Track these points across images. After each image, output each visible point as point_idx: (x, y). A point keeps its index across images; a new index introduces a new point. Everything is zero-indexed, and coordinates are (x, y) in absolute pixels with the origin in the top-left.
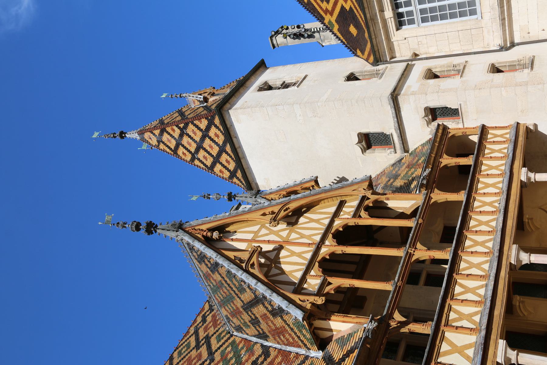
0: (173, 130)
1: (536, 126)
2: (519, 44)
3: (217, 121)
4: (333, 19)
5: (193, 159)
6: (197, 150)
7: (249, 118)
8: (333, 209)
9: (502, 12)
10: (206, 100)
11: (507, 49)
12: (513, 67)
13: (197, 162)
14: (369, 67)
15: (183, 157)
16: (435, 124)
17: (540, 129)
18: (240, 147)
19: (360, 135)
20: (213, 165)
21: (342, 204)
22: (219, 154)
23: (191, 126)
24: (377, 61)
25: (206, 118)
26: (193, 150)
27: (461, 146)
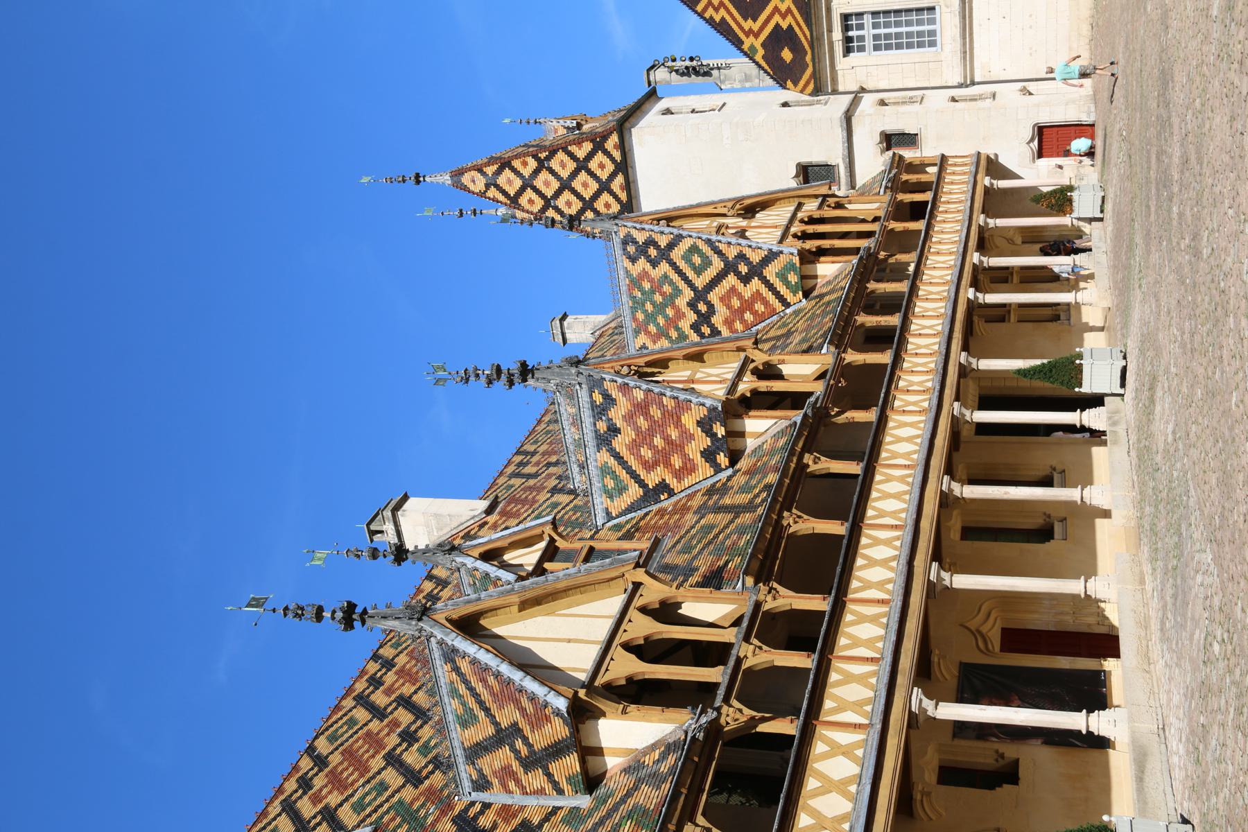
0: (525, 164)
1: (996, 156)
2: (979, 83)
4: (758, 43)
6: (558, 194)
8: (792, 208)
9: (964, 44)
10: (579, 126)
11: (967, 86)
12: (973, 99)
14: (806, 98)
15: (527, 207)
16: (890, 153)
17: (1001, 160)
18: (635, 181)
19: (798, 165)
21: (800, 206)
22: (596, 196)
23: (561, 155)
24: (817, 91)
25: (592, 141)
26: (549, 193)
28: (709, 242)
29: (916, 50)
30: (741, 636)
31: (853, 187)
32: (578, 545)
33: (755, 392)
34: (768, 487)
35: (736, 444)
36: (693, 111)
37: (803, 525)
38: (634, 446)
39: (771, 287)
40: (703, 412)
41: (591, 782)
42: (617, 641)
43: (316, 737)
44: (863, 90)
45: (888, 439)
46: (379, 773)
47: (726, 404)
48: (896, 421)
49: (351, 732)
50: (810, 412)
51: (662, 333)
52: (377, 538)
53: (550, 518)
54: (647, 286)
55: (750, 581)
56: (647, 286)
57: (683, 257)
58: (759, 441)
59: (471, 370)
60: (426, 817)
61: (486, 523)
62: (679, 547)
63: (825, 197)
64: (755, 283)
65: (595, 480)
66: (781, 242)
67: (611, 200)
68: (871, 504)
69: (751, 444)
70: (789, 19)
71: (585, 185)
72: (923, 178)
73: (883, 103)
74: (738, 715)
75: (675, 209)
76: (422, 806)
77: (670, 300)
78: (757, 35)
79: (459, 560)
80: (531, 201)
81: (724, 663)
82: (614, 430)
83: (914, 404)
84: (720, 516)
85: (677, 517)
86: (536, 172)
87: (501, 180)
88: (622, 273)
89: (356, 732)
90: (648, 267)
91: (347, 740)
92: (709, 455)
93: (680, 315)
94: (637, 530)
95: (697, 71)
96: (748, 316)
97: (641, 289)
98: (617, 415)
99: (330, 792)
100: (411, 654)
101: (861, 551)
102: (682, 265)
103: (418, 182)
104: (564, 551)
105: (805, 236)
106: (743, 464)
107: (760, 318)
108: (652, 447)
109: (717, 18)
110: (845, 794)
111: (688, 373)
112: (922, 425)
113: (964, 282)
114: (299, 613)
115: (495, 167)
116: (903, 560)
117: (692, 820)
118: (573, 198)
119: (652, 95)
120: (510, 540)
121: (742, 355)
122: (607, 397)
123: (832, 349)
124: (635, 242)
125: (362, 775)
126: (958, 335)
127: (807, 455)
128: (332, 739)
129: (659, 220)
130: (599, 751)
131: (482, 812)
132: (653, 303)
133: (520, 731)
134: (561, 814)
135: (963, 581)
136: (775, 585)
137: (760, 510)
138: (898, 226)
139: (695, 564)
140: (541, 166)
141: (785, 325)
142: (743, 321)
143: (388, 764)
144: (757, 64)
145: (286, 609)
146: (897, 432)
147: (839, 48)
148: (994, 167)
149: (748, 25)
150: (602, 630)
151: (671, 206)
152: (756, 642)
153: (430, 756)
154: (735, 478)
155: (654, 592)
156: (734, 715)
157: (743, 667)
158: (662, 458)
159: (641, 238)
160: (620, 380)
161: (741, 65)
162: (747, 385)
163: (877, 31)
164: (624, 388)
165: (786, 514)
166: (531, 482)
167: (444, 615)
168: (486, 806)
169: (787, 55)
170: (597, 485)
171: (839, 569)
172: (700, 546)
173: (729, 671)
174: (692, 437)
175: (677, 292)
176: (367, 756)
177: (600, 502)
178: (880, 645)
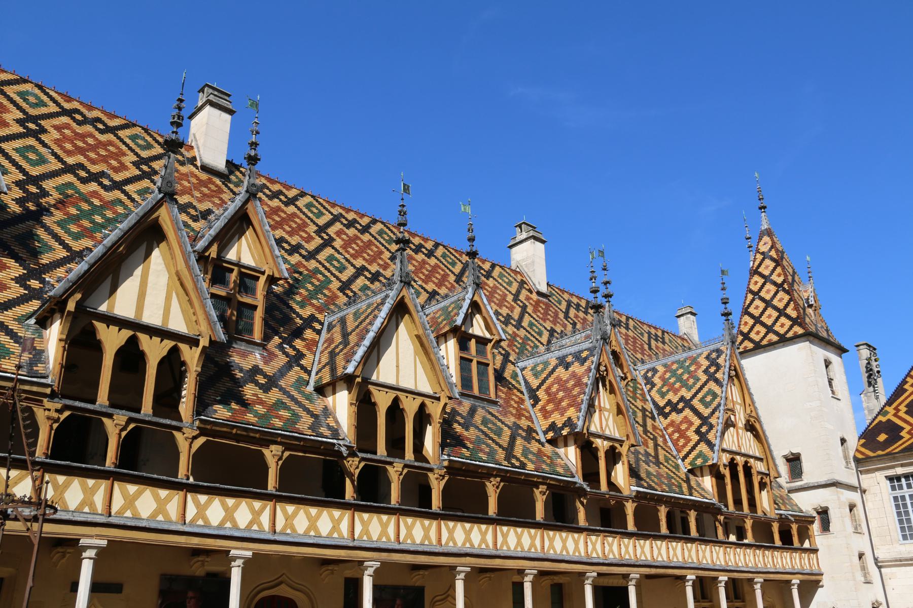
0: (779, 275)
1: (822, 586)
3: (798, 330)
4: (890, 416)
5: (751, 292)
6: (762, 299)
7: (802, 357)
8: (758, 455)
10: (810, 306)
12: (863, 568)
13: (750, 297)
14: (851, 454)
15: (753, 281)
16: (815, 514)
18: (775, 349)
20: (752, 316)
21: (761, 460)
22: (763, 325)
23: (787, 298)
24: (857, 461)
25: (798, 317)
26: (762, 294)
27: (804, 534)
28: (719, 405)
29: (898, 526)
30: (408, 463)
31: (789, 492)
32: (490, 356)
33: (597, 449)
34: (523, 466)
35: (561, 443)
36: (830, 381)
37: (492, 490)
38: (559, 380)
39: (693, 448)
40: (575, 420)
41: (321, 390)
42: (399, 393)
43: (382, 223)
44: (864, 492)
45: (564, 534)
46: (352, 265)
47: (580, 434)
48: (579, 538)
49: (384, 242)
50: (577, 485)
51: (665, 381)
52: (518, 229)
53: (504, 337)
54: (692, 368)
55: (446, 464)
56: (692, 368)
57: (710, 389)
58: (563, 456)
59: (595, 275)
60: (317, 299)
61: (530, 291)
62: (489, 417)
63: (768, 475)
64: (696, 438)
65: (541, 358)
66: (724, 450)
67: (762, 334)
68: (512, 529)
69: (561, 451)
70: (908, 436)
71: (770, 316)
72: (796, 539)
73: (852, 507)
74: (354, 467)
75: (745, 380)
76: (325, 295)
77: (684, 384)
78: (895, 415)
79: (470, 290)
80: (756, 283)
81: (388, 456)
82: (567, 366)
83: (594, 549)
84: (507, 439)
85: (514, 412)
86: (775, 283)
87: (768, 262)
88: (699, 351)
89: (383, 245)
90: (704, 368)
91: (378, 241)
92: (553, 427)
93: (676, 391)
94: (510, 389)
95: (871, 376)
96: (676, 435)
97: (691, 365)
98: (576, 368)
99: (343, 240)
100: (437, 266)
101: (476, 526)
102: (705, 389)
103: (760, 208)
104: (485, 349)
105: (732, 465)
106: (548, 448)
107: (675, 443)
108: (558, 390)
109: (906, 387)
110: (308, 529)
111: (608, 406)
112: (577, 554)
113: (700, 572)
114: (402, 213)
115: (775, 256)
116: (469, 551)
117: (286, 449)
118: (760, 310)
119: (841, 350)
120: (487, 317)
121: (625, 438)
122: (585, 359)
123: (634, 494)
124: (718, 357)
125: (352, 256)
126: (653, 571)
127: (545, 487)
128: (381, 233)
129: (735, 370)
130: (334, 393)
131: (314, 330)
132: (682, 374)
133: (345, 347)
134: (305, 376)
135: (460, 586)
136: (446, 478)
137: (506, 463)
138: (749, 524)
139: (472, 429)
140: (779, 286)
141: (667, 460)
142: (673, 432)
143: (358, 269)
144: (876, 417)
145: (403, 206)
146: (570, 539)
147: (891, 472)
148: (810, 586)
149: (903, 408)
150: (407, 383)
151: (748, 376)
152: (405, 471)
153: (359, 293)
154: (537, 444)
155: (435, 410)
156: (354, 465)
157: (388, 467)
158: (552, 398)
159: (721, 361)
160: (593, 367)
161: (876, 406)
162: (602, 445)
163: (907, 498)
164: (589, 370)
165: (498, 479)
166: (561, 315)
167: (405, 294)
168: (319, 332)
169: (882, 437)
170: (538, 360)
171: (459, 514)
172: (485, 429)
173: (383, 459)
174: (562, 415)
175: (689, 388)
176: (365, 255)
177: (530, 363)
178: (409, 541)
